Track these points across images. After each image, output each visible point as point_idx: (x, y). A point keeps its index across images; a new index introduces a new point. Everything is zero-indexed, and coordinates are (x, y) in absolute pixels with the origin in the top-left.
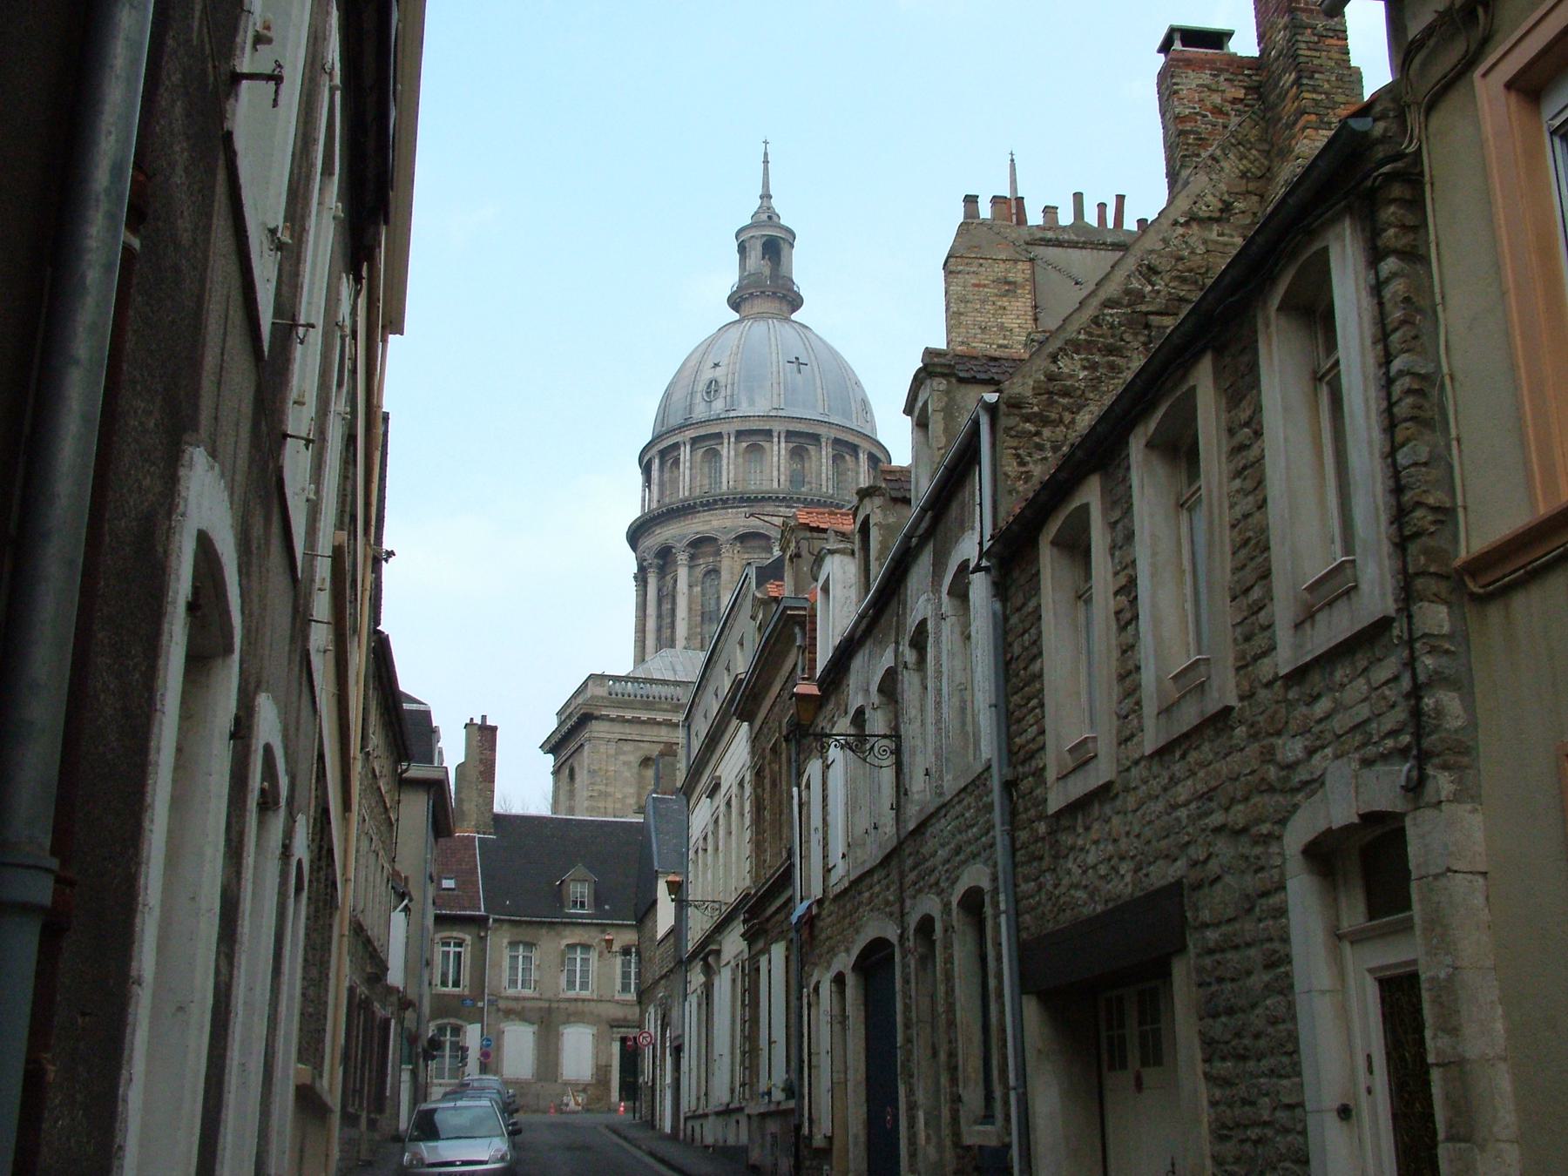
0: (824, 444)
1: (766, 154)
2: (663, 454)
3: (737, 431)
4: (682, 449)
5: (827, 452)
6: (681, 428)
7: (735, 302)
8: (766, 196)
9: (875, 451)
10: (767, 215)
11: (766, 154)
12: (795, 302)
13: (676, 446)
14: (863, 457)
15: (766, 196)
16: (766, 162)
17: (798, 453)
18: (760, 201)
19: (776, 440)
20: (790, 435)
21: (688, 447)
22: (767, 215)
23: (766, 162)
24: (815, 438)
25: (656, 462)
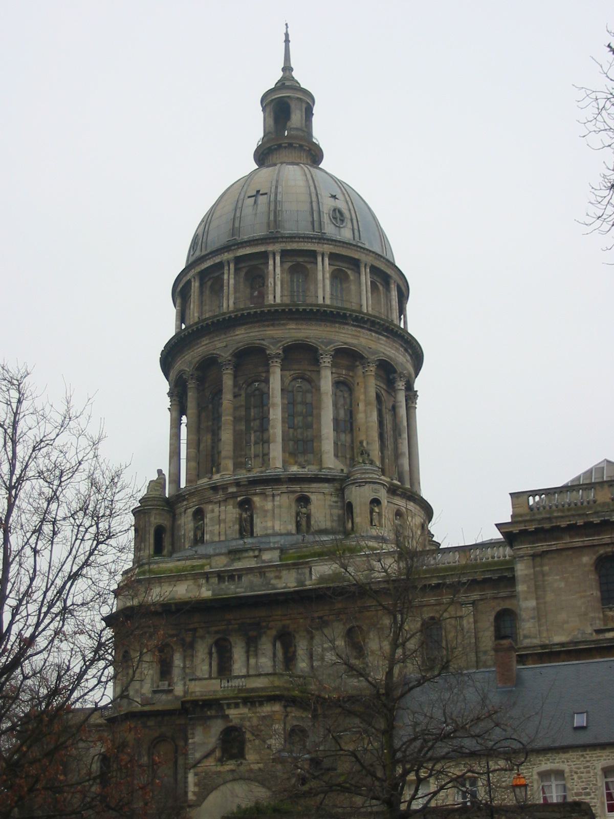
0: (363, 269)
1: (287, 35)
2: (203, 275)
3: (282, 250)
4: (226, 268)
5: (366, 278)
6: (226, 248)
7: (263, 156)
8: (287, 69)
9: (401, 283)
10: (287, 83)
11: (287, 35)
12: (315, 155)
13: (220, 266)
14: (393, 287)
15: (287, 69)
16: (287, 41)
17: (338, 277)
18: (281, 73)
19: (319, 259)
20: (333, 257)
21: (232, 266)
22: (287, 83)
23: (287, 41)
24: (355, 264)
25: (195, 285)
